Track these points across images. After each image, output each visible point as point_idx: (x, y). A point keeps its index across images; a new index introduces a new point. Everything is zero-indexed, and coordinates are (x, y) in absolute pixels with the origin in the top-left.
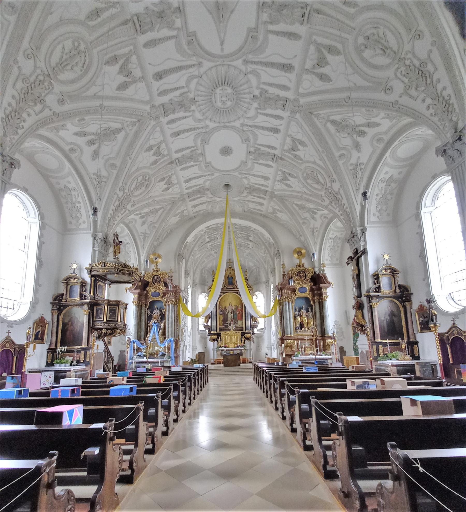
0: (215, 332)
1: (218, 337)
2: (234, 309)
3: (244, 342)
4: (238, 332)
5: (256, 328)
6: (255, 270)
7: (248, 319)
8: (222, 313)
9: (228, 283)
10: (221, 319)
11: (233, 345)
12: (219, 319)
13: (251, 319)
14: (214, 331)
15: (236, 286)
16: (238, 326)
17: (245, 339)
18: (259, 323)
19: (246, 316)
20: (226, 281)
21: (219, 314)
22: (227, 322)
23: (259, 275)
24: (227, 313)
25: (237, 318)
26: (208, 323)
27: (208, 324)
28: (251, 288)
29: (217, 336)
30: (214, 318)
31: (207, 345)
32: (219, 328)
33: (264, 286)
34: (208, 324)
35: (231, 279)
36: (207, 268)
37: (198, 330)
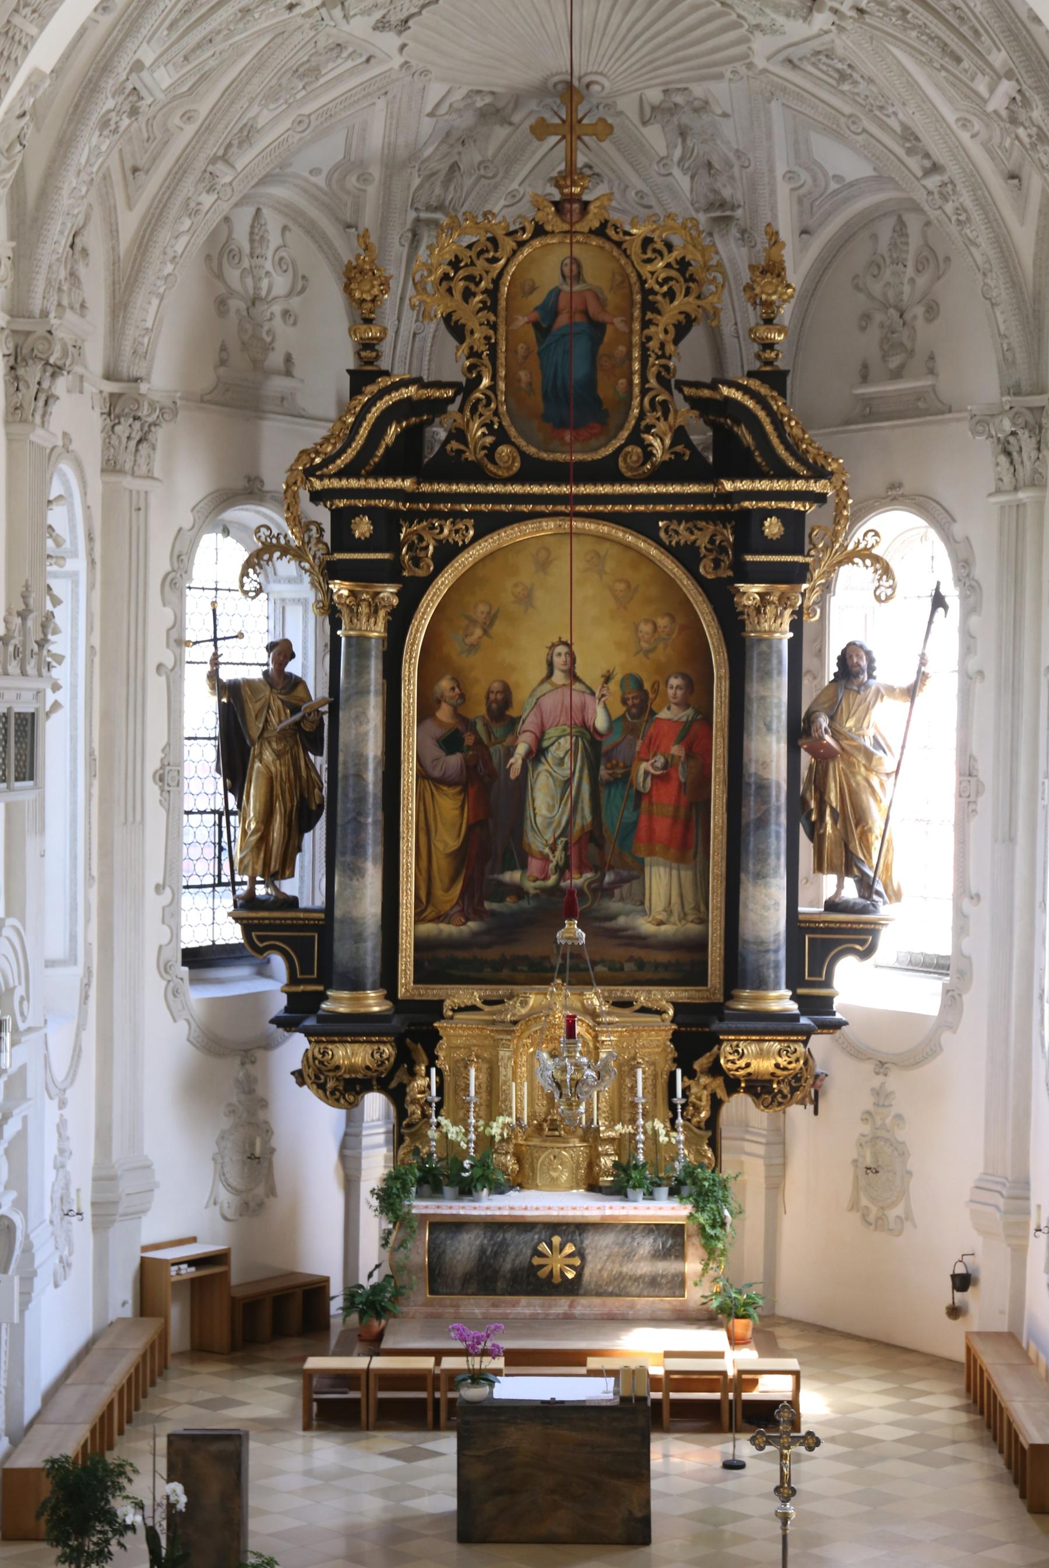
0: (374, 1002)
1: (405, 1060)
2: (601, 722)
3: (712, 1123)
4: (642, 996)
5: (866, 954)
6: (885, 230)
7: (762, 856)
8: (455, 761)
9: (537, 402)
10: (448, 840)
11: (575, 1149)
12: (425, 829)
13: (806, 847)
14: (356, 984)
15: (635, 438)
16: (645, 926)
17: (720, 1081)
18: (896, 896)
19: (750, 812)
20: (523, 375)
21: (422, 775)
22: (513, 876)
23: (932, 311)
24: (516, 761)
25: (629, 830)
26: (286, 868)
27: (289, 887)
28: (816, 487)
29: (388, 1050)
30: (359, 827)
31: (266, 1131)
32: (421, 945)
33: (984, 450)
34: (289, 887)
35: (580, 347)
36: (279, 192)
37: (165, 969)
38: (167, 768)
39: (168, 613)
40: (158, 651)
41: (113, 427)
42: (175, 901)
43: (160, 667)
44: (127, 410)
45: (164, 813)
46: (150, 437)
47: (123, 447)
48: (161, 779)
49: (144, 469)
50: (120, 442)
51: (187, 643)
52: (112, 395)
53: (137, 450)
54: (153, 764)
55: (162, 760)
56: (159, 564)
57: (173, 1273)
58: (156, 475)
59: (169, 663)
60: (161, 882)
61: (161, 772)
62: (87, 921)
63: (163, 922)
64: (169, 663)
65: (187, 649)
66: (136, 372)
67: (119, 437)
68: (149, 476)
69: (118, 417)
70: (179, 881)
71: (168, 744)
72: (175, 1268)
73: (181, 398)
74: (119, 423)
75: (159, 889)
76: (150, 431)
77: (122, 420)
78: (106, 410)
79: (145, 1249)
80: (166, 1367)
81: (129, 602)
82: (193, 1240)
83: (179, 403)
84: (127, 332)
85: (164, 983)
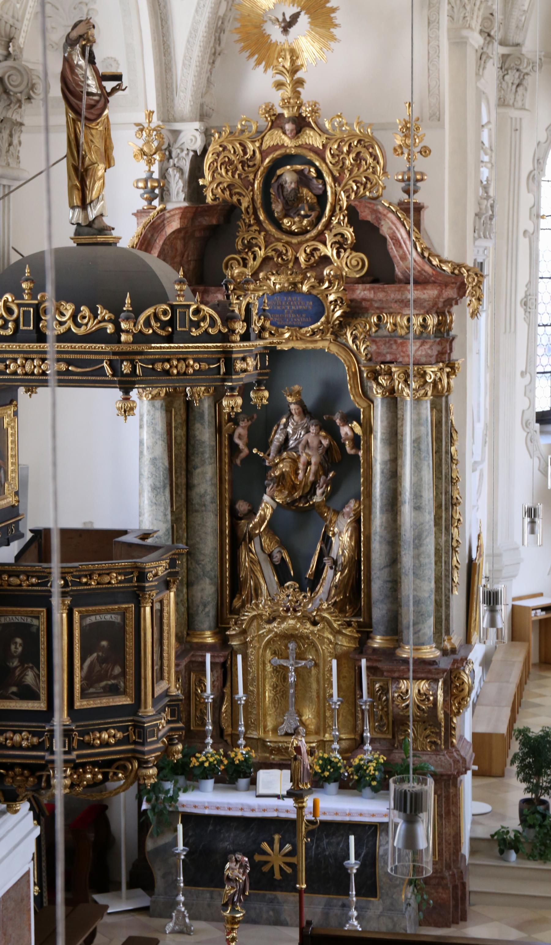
37: (526, 425)
38: (529, 297)
39: (531, 196)
40: (526, 224)
41: (504, 76)
42: (532, 381)
43: (525, 232)
44: (512, 65)
45: (526, 326)
46: (525, 82)
47: (509, 90)
48: (525, 304)
49: (519, 104)
50: (508, 86)
51: (543, 217)
52: (503, 55)
53: (516, 91)
54: (521, 295)
55: (526, 292)
56: (527, 166)
57: (533, 615)
58: (527, 107)
59: (531, 230)
60: (524, 370)
61: (525, 299)
62: (486, 393)
63: (525, 395)
64: (531, 230)
65: (542, 220)
66: (518, 40)
67: (507, 83)
68: (523, 108)
69: (507, 70)
70: (535, 369)
71: (530, 282)
72: (533, 612)
73: (544, 56)
74: (507, 74)
75: (523, 374)
76: (524, 78)
77: (510, 71)
78: (500, 66)
79: (514, 599)
80: (529, 673)
81: (509, 191)
82: (541, 595)
83: (543, 59)
84: (514, 13)
85: (525, 434)
